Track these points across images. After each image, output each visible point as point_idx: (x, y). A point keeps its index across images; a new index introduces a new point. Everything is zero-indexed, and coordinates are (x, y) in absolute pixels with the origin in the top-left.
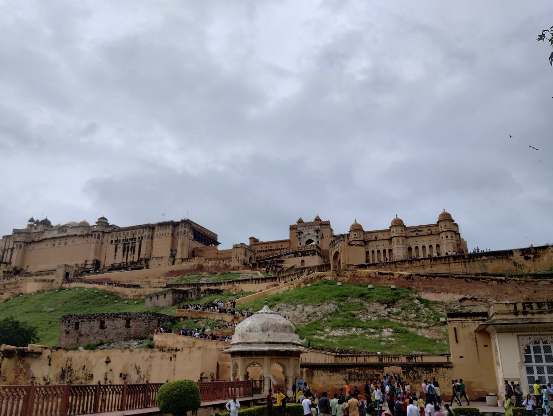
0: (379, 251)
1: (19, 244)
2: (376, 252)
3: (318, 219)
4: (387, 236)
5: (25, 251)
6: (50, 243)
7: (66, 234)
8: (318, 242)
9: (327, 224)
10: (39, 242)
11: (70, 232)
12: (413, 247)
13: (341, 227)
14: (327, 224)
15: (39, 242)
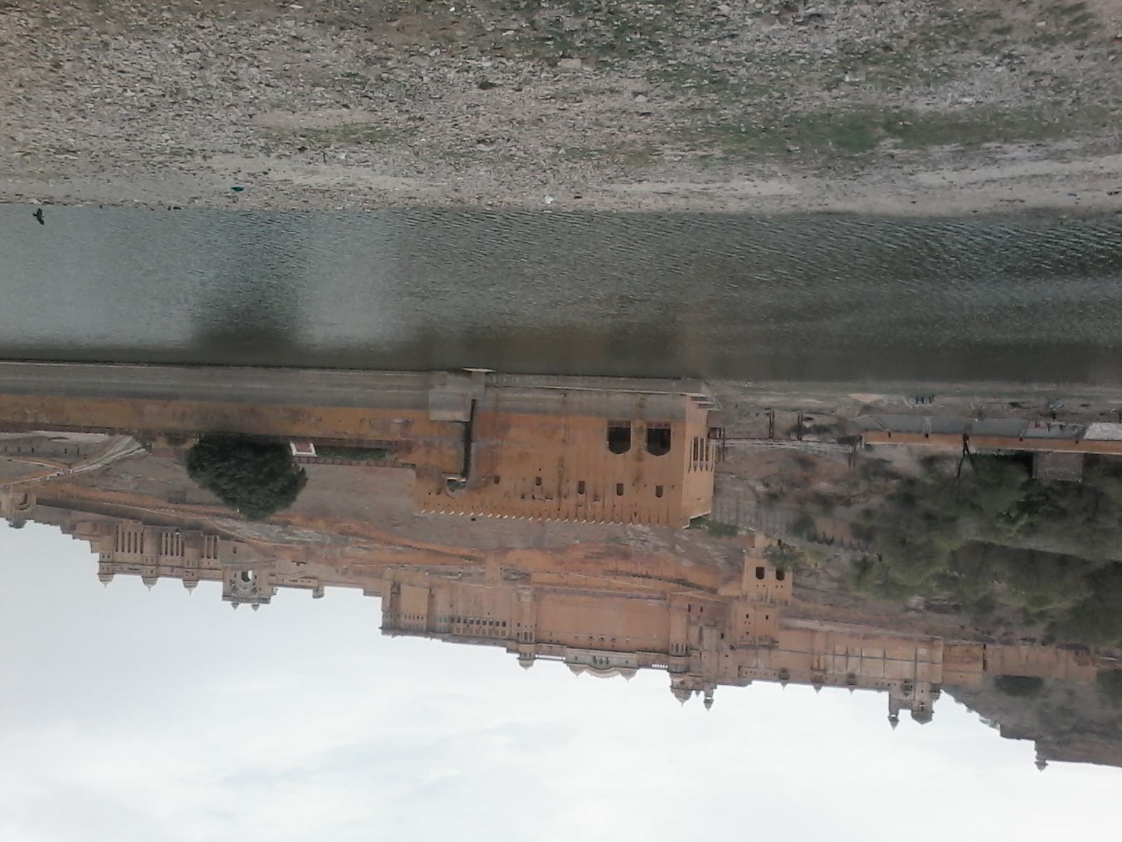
0: (172, 554)
1: (674, 652)
2: (175, 553)
3: (235, 605)
4: (163, 570)
5: (669, 640)
6: (621, 643)
7: (593, 653)
8: (235, 576)
9: (226, 596)
10: (645, 650)
11: (586, 656)
12: (139, 552)
13: (211, 589)
14: (226, 596)
15: (645, 650)
